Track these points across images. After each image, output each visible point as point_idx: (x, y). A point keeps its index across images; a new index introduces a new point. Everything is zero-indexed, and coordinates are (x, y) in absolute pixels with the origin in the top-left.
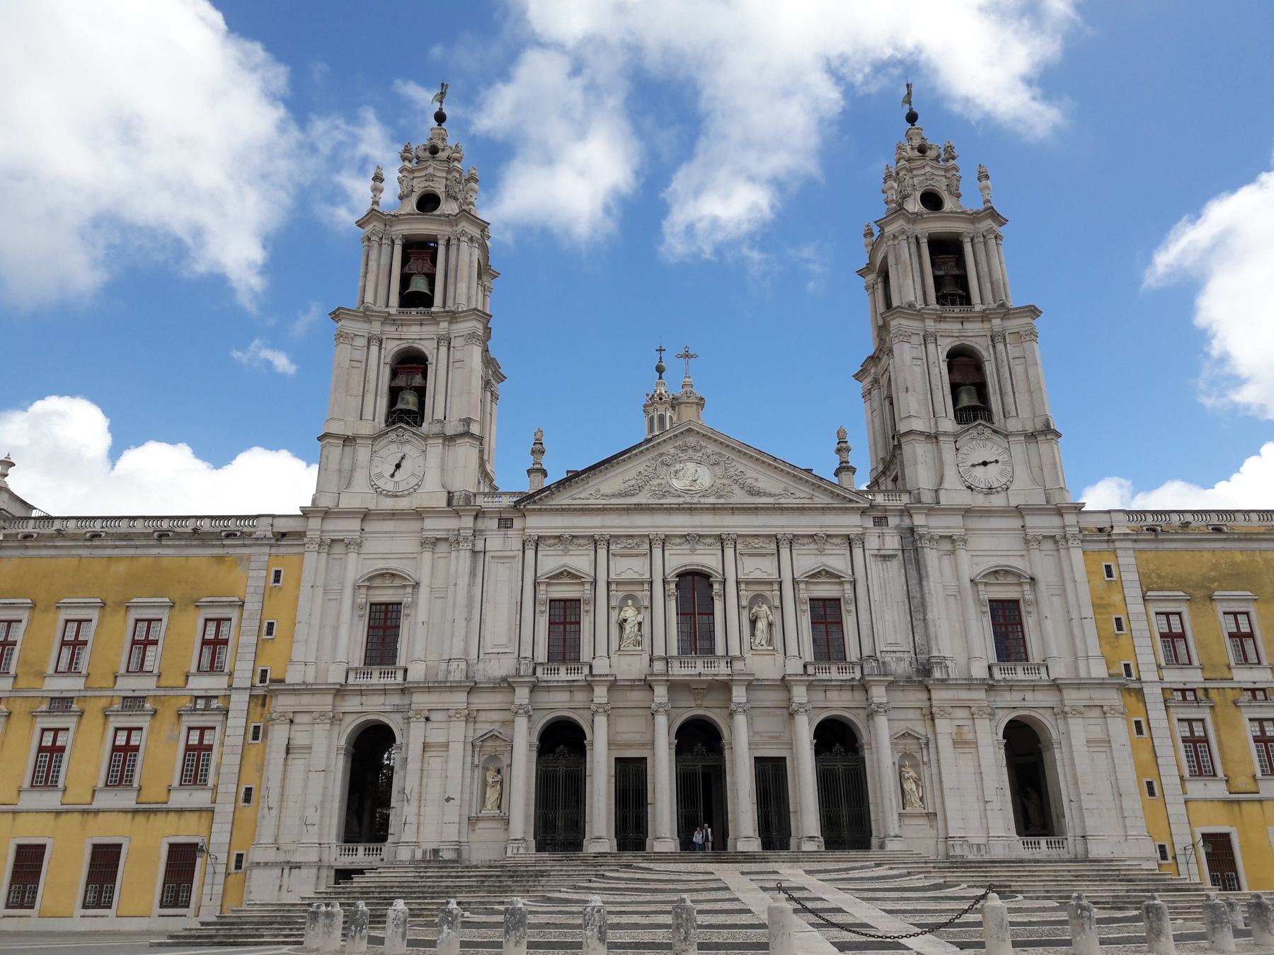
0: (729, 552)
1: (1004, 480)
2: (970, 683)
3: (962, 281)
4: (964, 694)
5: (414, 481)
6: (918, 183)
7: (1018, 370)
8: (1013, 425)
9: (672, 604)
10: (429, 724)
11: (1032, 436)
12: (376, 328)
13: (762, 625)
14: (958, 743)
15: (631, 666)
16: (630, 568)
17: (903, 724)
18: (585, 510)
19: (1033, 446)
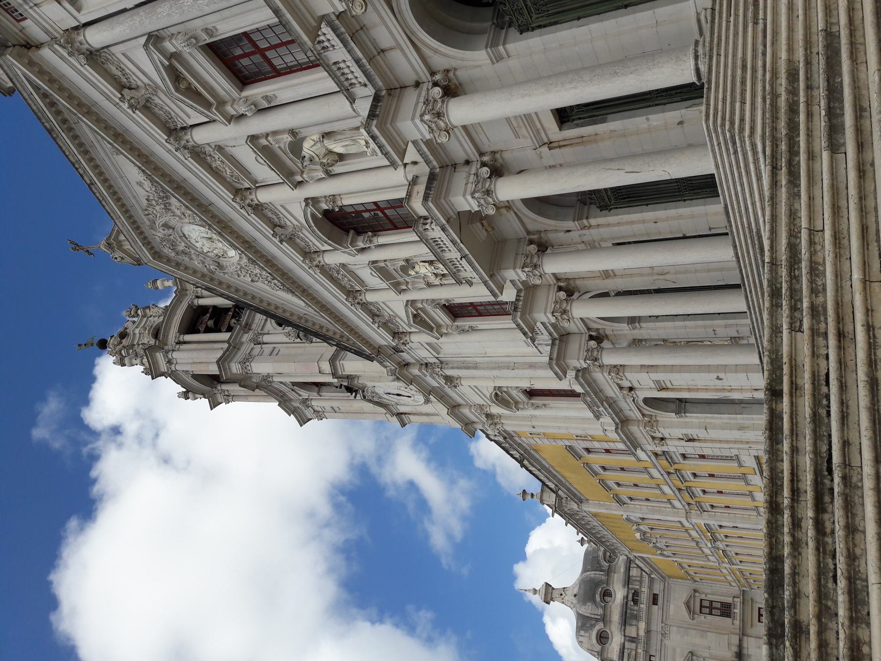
10: (636, 385)
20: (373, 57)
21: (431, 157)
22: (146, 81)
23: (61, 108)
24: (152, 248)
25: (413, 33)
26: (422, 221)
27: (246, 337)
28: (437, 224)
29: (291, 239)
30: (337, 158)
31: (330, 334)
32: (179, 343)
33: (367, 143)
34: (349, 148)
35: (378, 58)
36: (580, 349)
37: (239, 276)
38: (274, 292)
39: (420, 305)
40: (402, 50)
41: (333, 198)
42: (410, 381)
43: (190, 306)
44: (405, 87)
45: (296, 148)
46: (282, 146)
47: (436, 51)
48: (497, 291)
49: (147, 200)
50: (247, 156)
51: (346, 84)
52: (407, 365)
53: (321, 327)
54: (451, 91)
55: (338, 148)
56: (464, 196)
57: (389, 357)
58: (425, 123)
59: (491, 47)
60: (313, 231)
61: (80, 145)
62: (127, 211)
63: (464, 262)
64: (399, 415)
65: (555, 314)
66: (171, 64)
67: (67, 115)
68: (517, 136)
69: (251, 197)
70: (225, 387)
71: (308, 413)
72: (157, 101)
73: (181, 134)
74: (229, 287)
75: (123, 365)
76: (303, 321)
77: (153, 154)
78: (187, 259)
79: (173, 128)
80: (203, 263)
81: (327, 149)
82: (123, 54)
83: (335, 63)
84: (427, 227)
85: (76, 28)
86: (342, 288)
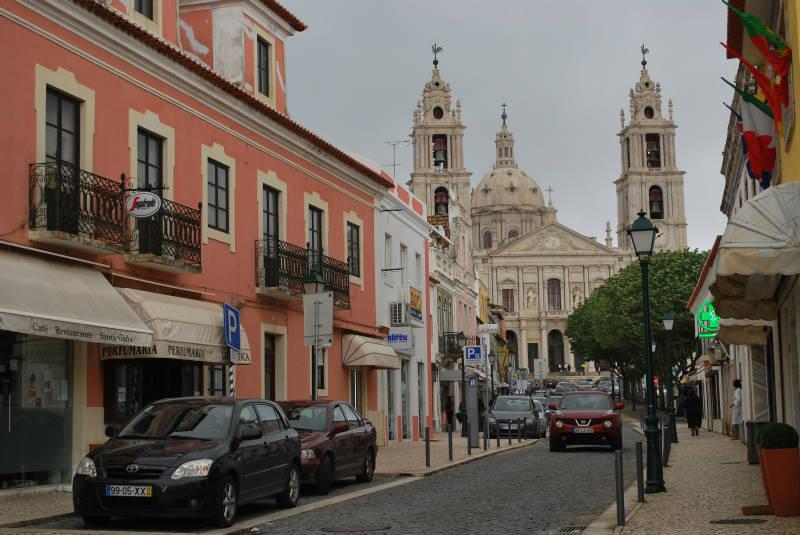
0: (566, 272)
3: (657, 154)
6: (643, 104)
7: (675, 196)
8: (671, 221)
12: (429, 180)
15: (533, 312)
16: (531, 278)
18: (515, 256)
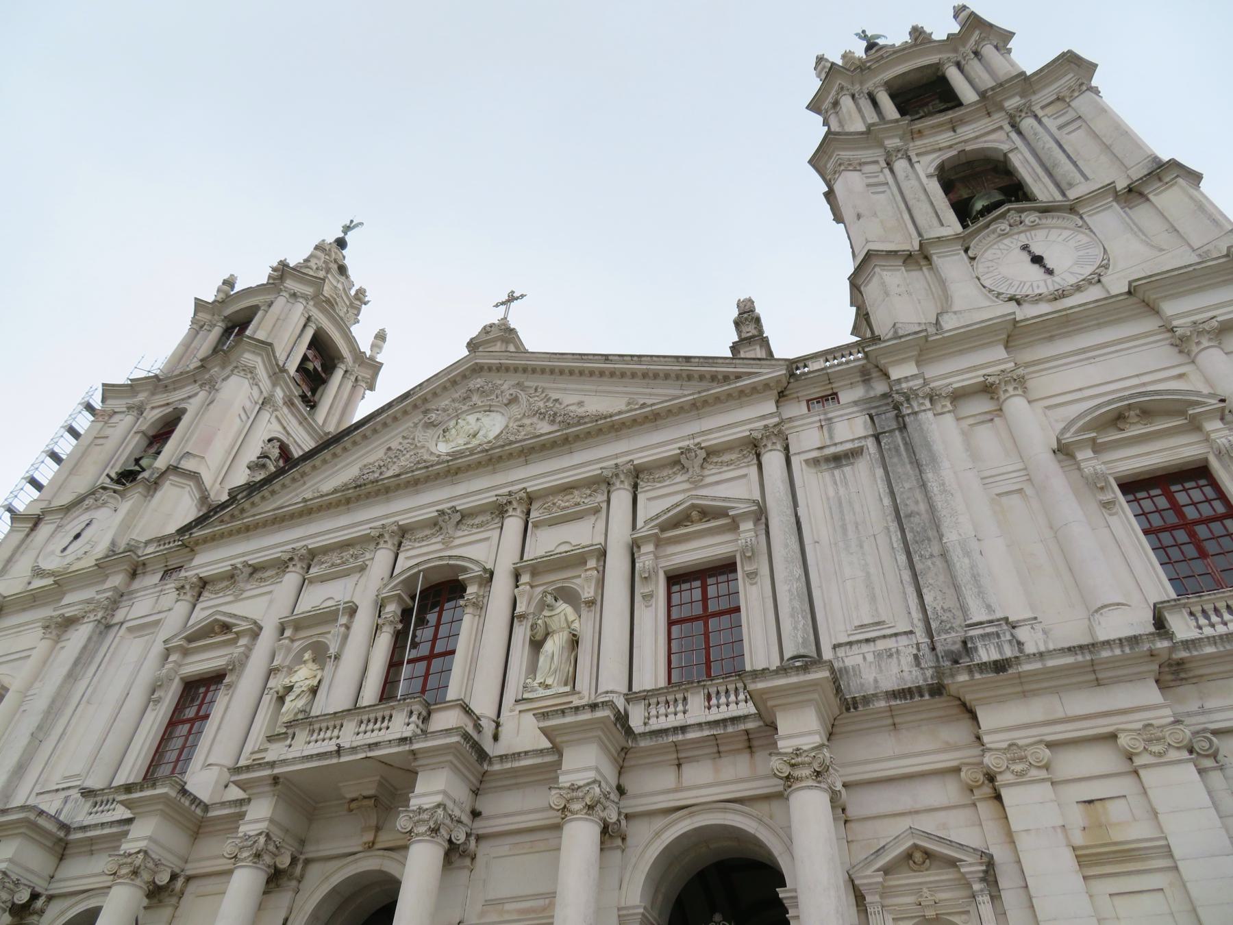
1: (1087, 271)
2: (1091, 664)
4: (1083, 703)
5: (87, 548)
9: (385, 641)
11: (1133, 194)
13: (554, 645)
14: (1099, 859)
17: (904, 824)
19: (1141, 213)
20: (678, 749)
21: (508, 765)
22: (708, 480)
23: (715, 384)
24: (490, 369)
25: (691, 814)
26: (424, 713)
27: (279, 394)
28: (416, 735)
29: (435, 525)
30: (538, 638)
31: (257, 498)
32: (309, 319)
33: (547, 687)
34: (549, 660)
35: (674, 756)
36: (27, 870)
37: (404, 438)
38: (360, 465)
39: (243, 641)
40: (676, 790)
41: (480, 606)
42: (102, 567)
43: (341, 358)
44: (620, 773)
45: (567, 595)
46: (577, 581)
47: (658, 834)
48: (244, 776)
49: (556, 400)
50: (580, 535)
51: (653, 701)
52: (134, 575)
53: (273, 493)
54: (609, 834)
55: (550, 646)
56: (445, 793)
57: (165, 557)
58: (588, 784)
59: (643, 915)
60: (441, 558)
61: (656, 376)
62: (552, 372)
63: (330, 746)
64: (36, 521)
65: (141, 856)
66: (727, 515)
67: (704, 384)
68: (489, 903)
69: (519, 510)
70: (217, 331)
71: (118, 404)
72: (679, 478)
73: (632, 481)
74: (395, 419)
75: (317, 248)
76: (297, 476)
77: (618, 439)
78: (456, 396)
79: (641, 476)
80: (445, 410)
81: (554, 632)
82: (745, 476)
83: (685, 699)
84: (414, 718)
85: (787, 448)
86: (326, 550)
